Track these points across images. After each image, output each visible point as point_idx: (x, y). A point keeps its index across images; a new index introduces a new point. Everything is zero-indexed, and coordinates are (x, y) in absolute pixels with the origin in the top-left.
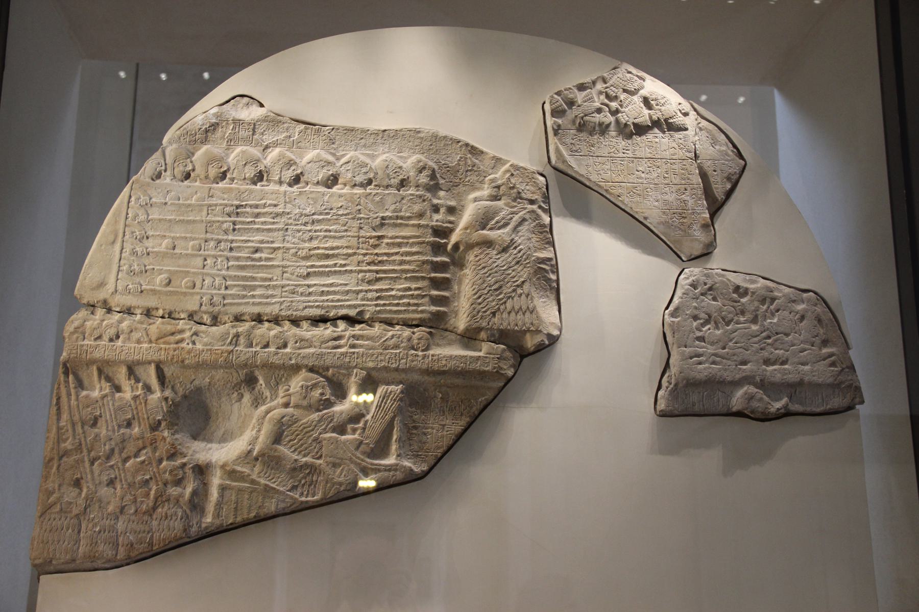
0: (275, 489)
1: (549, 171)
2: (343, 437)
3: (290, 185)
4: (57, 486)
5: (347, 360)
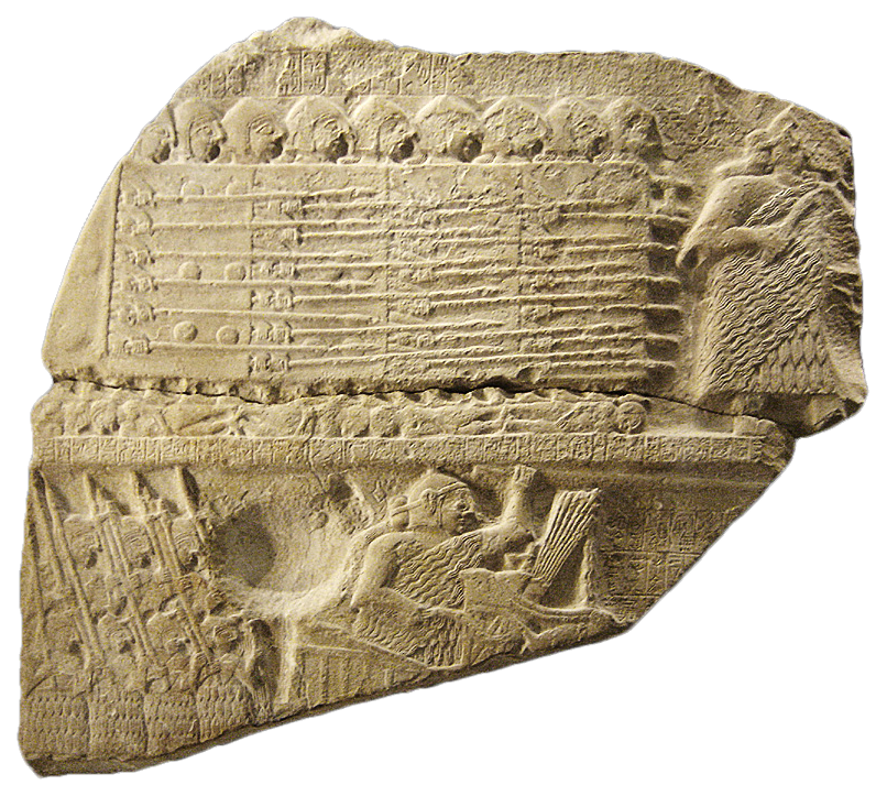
0: (387, 653)
2: (498, 573)
3: (395, 158)
4: (45, 652)
5: (503, 450)
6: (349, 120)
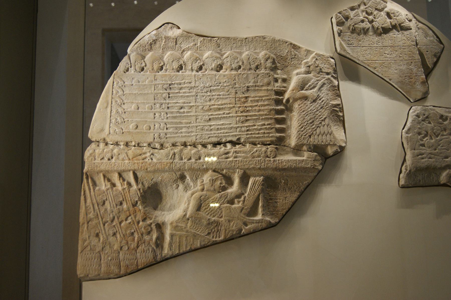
1: (336, 56)
3: (197, 71)
4: (87, 237)
5: (233, 164)
6: (183, 59)
